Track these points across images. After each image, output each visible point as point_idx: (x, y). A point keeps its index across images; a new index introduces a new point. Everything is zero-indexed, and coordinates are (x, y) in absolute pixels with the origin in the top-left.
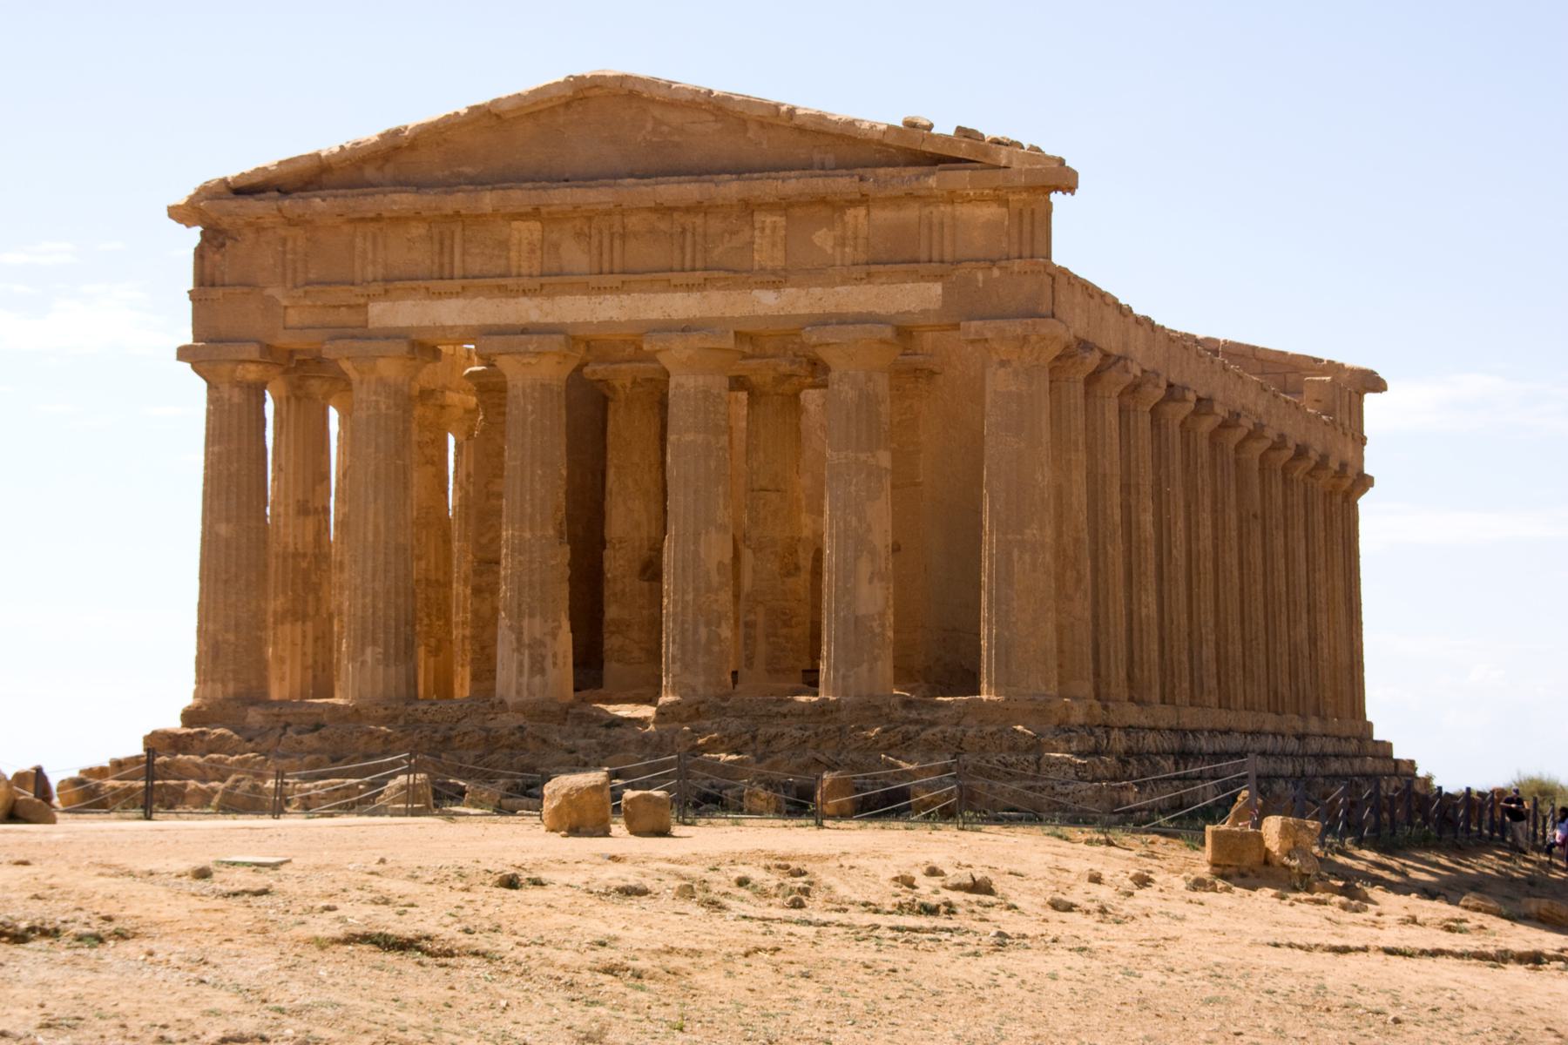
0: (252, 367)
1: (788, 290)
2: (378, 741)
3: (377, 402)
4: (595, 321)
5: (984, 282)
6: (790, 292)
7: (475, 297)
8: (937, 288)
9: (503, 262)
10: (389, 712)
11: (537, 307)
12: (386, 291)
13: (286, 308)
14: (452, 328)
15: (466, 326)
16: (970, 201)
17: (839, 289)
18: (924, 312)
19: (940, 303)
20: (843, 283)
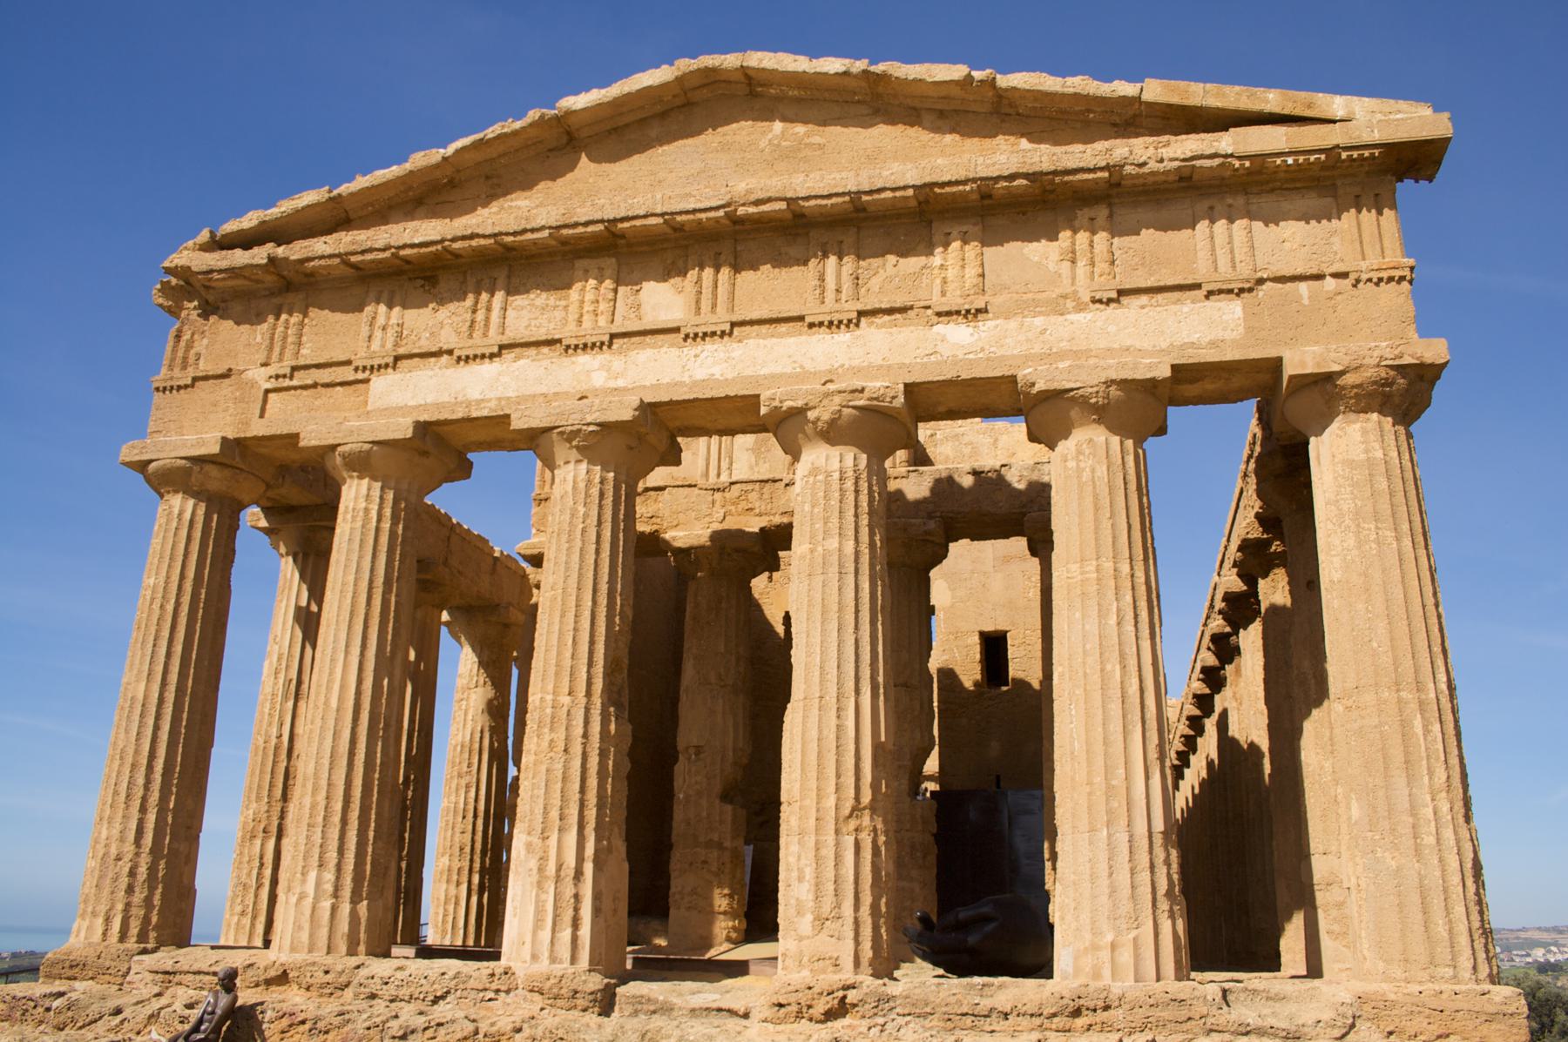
0: (213, 471)
1: (989, 323)
2: (301, 1028)
3: (367, 510)
4: (686, 379)
5: (1309, 298)
6: (987, 326)
7: (518, 358)
8: (1232, 311)
9: (559, 314)
10: (329, 978)
11: (601, 367)
12: (397, 359)
13: (267, 391)
14: (479, 402)
15: (499, 399)
16: (1272, 190)
17: (1068, 317)
18: (1213, 344)
19: (1241, 329)
20: (1080, 308)
